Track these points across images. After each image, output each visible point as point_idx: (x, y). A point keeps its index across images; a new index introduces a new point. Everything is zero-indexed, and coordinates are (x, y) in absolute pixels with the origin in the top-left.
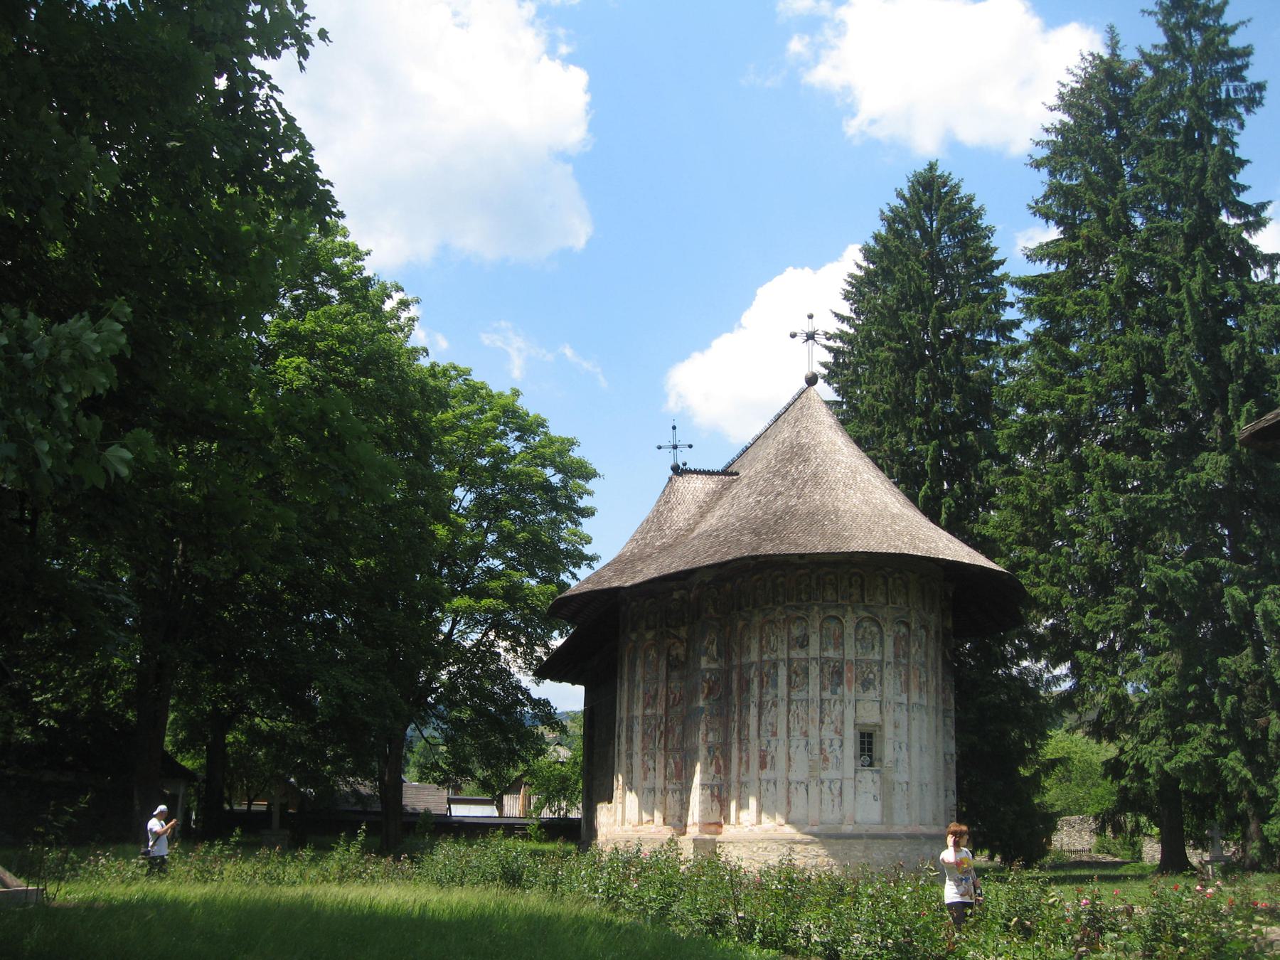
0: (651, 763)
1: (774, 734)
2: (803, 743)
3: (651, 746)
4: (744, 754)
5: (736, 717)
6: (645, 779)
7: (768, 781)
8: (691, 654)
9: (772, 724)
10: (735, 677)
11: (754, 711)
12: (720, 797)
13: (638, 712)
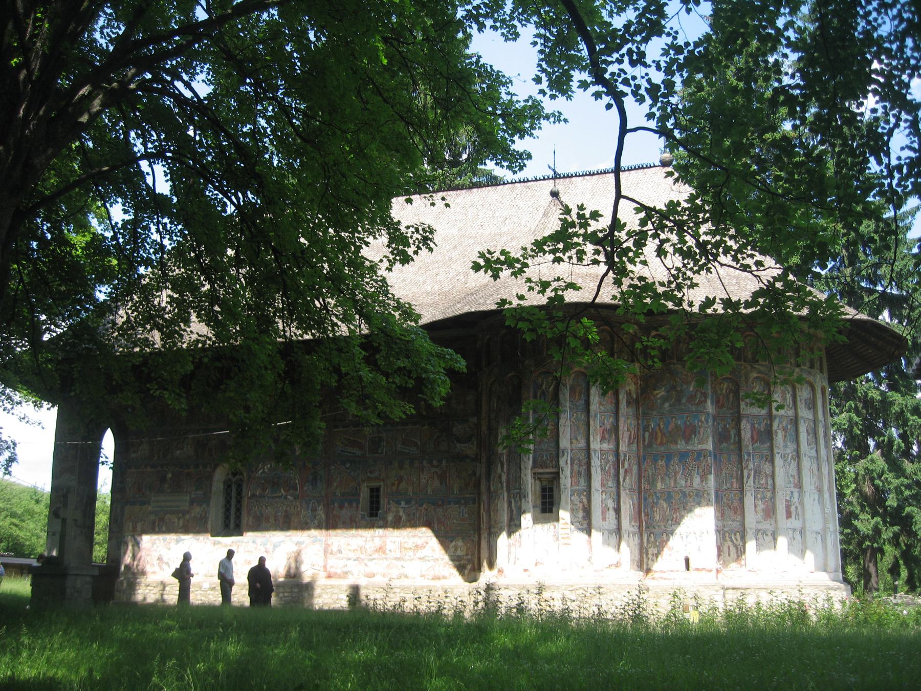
0: (611, 504)
1: (799, 486)
2: (817, 497)
3: (610, 484)
4: (760, 502)
5: (751, 466)
6: (604, 519)
7: (794, 530)
8: (661, 393)
9: (793, 476)
10: (745, 426)
11: (778, 461)
12: (731, 541)
13: (595, 445)
